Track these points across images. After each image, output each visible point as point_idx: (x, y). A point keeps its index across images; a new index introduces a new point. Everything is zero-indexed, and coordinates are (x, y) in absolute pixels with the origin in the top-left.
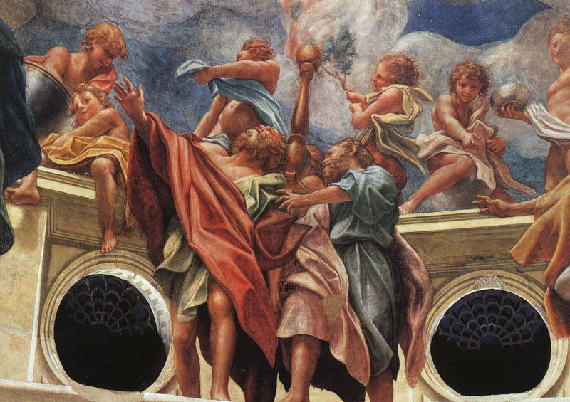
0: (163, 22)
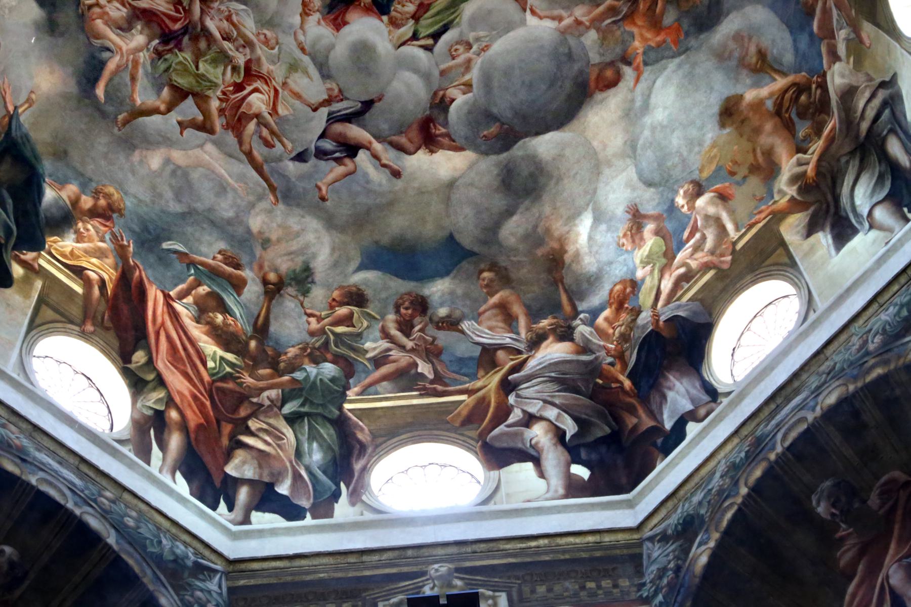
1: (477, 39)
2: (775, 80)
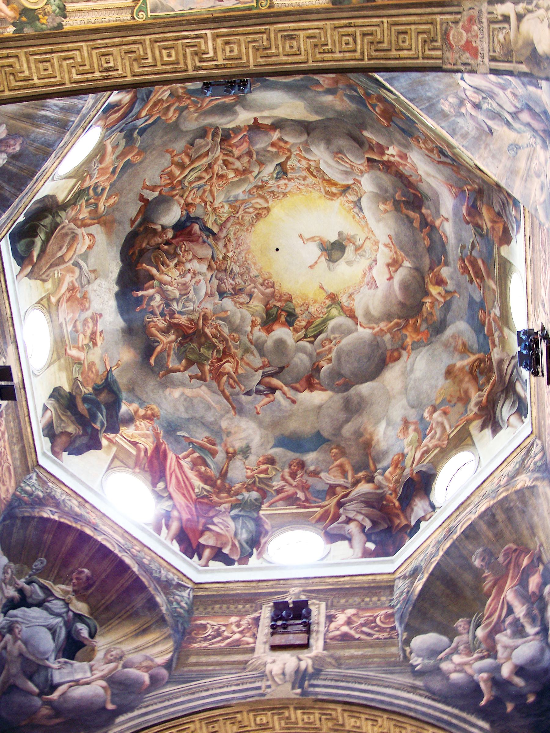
0: (176, 416)
1: (335, 338)
2: (469, 357)
